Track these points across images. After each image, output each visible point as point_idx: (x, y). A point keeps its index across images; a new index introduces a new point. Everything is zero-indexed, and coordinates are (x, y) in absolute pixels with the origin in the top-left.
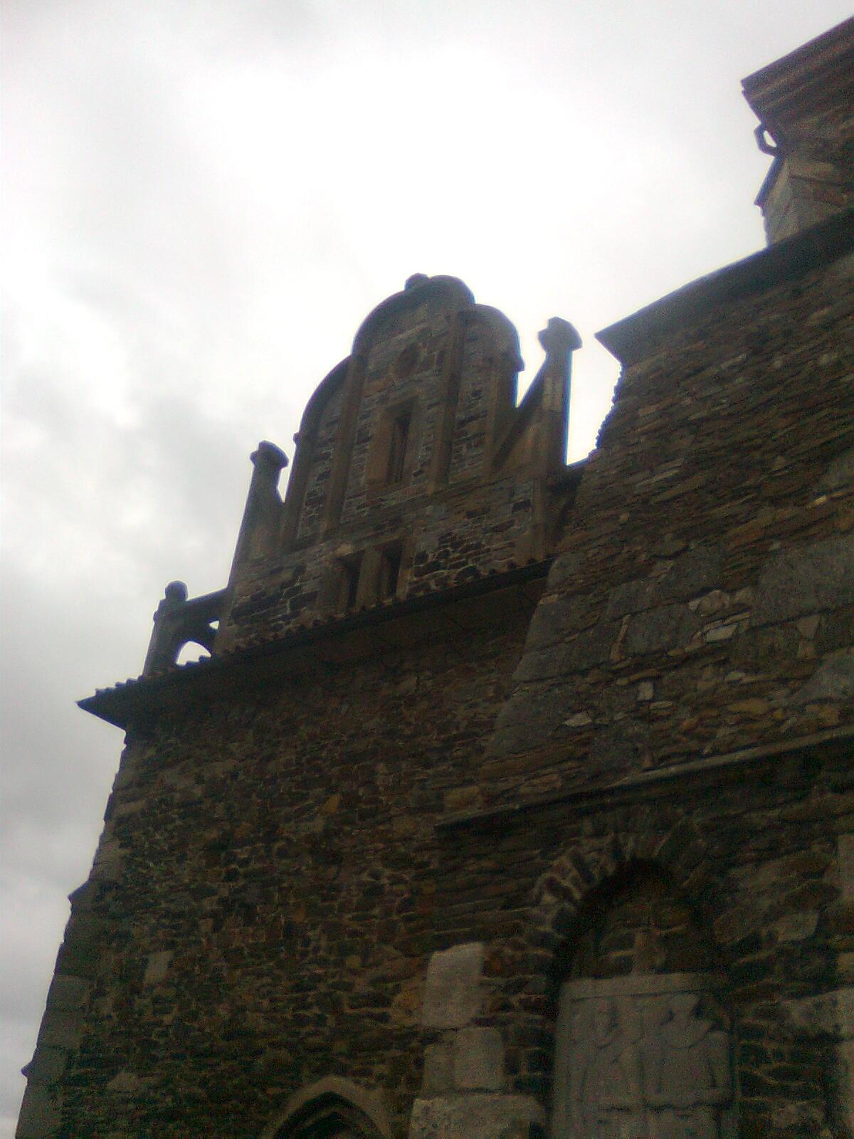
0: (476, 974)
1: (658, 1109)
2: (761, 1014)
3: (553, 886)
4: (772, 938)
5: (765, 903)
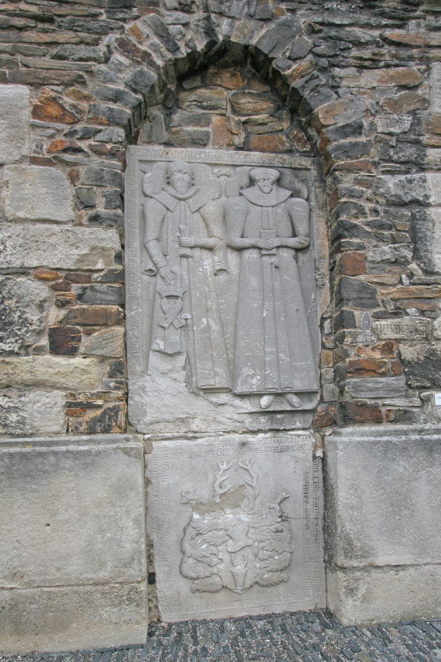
2: (358, 182)
4: (373, 127)
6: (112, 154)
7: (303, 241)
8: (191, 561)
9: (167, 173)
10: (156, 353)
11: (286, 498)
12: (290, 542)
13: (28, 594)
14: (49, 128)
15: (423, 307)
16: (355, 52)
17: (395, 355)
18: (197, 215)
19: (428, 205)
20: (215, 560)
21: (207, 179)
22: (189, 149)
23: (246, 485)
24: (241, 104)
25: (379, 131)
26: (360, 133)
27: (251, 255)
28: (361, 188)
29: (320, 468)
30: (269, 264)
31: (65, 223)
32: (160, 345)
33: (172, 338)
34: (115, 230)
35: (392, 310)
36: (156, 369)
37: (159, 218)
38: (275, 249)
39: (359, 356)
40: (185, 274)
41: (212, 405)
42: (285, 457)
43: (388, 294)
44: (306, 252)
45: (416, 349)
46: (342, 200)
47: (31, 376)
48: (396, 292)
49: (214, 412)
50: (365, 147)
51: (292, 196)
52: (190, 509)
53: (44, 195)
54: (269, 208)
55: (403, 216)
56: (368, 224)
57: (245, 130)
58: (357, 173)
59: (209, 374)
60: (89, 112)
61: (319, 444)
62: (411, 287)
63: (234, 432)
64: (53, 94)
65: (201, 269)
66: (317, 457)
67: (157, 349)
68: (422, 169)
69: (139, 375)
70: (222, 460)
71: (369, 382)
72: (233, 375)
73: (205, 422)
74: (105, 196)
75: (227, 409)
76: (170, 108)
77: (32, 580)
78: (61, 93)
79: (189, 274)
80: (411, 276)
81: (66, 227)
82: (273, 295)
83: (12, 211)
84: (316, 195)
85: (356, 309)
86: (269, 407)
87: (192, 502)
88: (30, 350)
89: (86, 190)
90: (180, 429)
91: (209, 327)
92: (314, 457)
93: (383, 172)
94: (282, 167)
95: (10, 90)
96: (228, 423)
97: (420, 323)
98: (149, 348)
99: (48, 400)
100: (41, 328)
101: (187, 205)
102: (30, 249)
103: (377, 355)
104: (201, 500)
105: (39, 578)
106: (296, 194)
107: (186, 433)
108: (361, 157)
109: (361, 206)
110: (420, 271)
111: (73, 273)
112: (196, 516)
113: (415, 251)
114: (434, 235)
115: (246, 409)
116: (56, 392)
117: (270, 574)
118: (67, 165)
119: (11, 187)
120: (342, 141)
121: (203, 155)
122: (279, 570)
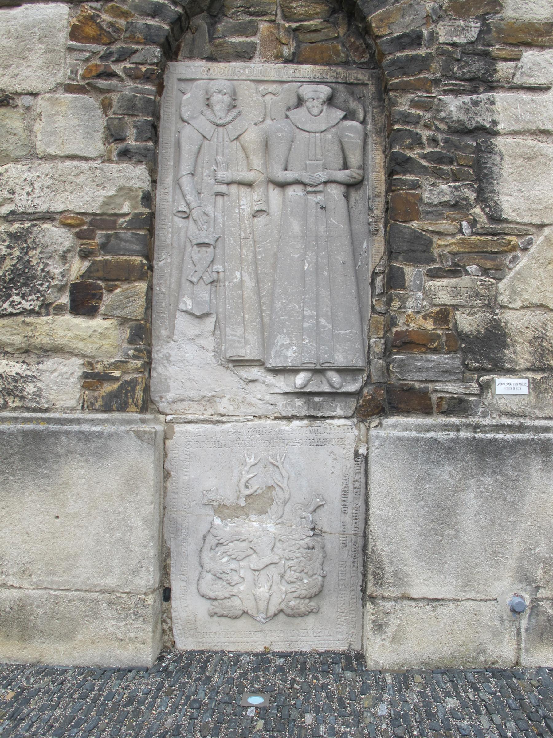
0: (63, 38)
2: (414, 104)
4: (433, 36)
6: (147, 78)
7: (355, 175)
8: (209, 576)
10: (183, 313)
11: (320, 506)
12: (323, 562)
13: (36, 596)
14: (85, 50)
15: (486, 264)
17: (451, 325)
18: (236, 144)
20: (235, 578)
21: (250, 99)
23: (275, 486)
24: (292, 7)
25: (441, 42)
26: (419, 45)
27: (295, 192)
28: (418, 112)
29: (363, 469)
30: (314, 204)
31: (94, 159)
32: (187, 303)
33: (200, 295)
34: (144, 166)
35: (450, 266)
36: (182, 333)
37: (195, 148)
38: (321, 185)
39: (408, 325)
40: (219, 215)
41: (242, 382)
42: (322, 452)
43: (446, 246)
44: (359, 189)
45: (476, 319)
46: (396, 127)
47: (50, 340)
48: (454, 243)
49: (243, 390)
50: (428, 58)
51: (345, 118)
52: (212, 513)
53: (75, 127)
54: (317, 134)
55: (467, 146)
56: (424, 157)
57: (296, 38)
58: (413, 93)
59: (239, 342)
60: (126, 30)
61: (363, 438)
62: (473, 237)
63: (266, 417)
64: (91, 12)
65: (237, 211)
66: (360, 455)
67: (185, 309)
68: (491, 87)
69: (164, 340)
70: (249, 452)
71: (418, 360)
72: (266, 344)
73: (234, 403)
74: (136, 126)
75: (258, 388)
78: (99, 10)
79: (223, 217)
80: (473, 223)
81: (95, 164)
82: (317, 243)
83: (43, 147)
84: (373, 116)
85: (407, 265)
86: (305, 386)
87: (214, 504)
89: (117, 121)
90: (205, 410)
91: (242, 281)
92: (356, 455)
93: (446, 92)
94: (335, 83)
95: (50, 10)
96: (259, 406)
97: (482, 285)
98: (176, 308)
99: (65, 369)
100: (63, 283)
101: (225, 132)
102: (57, 190)
103: (429, 325)
104: (224, 503)
106: (350, 115)
107: (212, 415)
108: (419, 73)
109: (417, 134)
110: (484, 217)
111: (98, 218)
112: (217, 521)
113: (480, 192)
114: (502, 172)
115: (279, 388)
116: (74, 359)
117: (298, 601)
118: (101, 92)
119: (43, 120)
120: (399, 54)
121: (247, 71)
122: (308, 597)
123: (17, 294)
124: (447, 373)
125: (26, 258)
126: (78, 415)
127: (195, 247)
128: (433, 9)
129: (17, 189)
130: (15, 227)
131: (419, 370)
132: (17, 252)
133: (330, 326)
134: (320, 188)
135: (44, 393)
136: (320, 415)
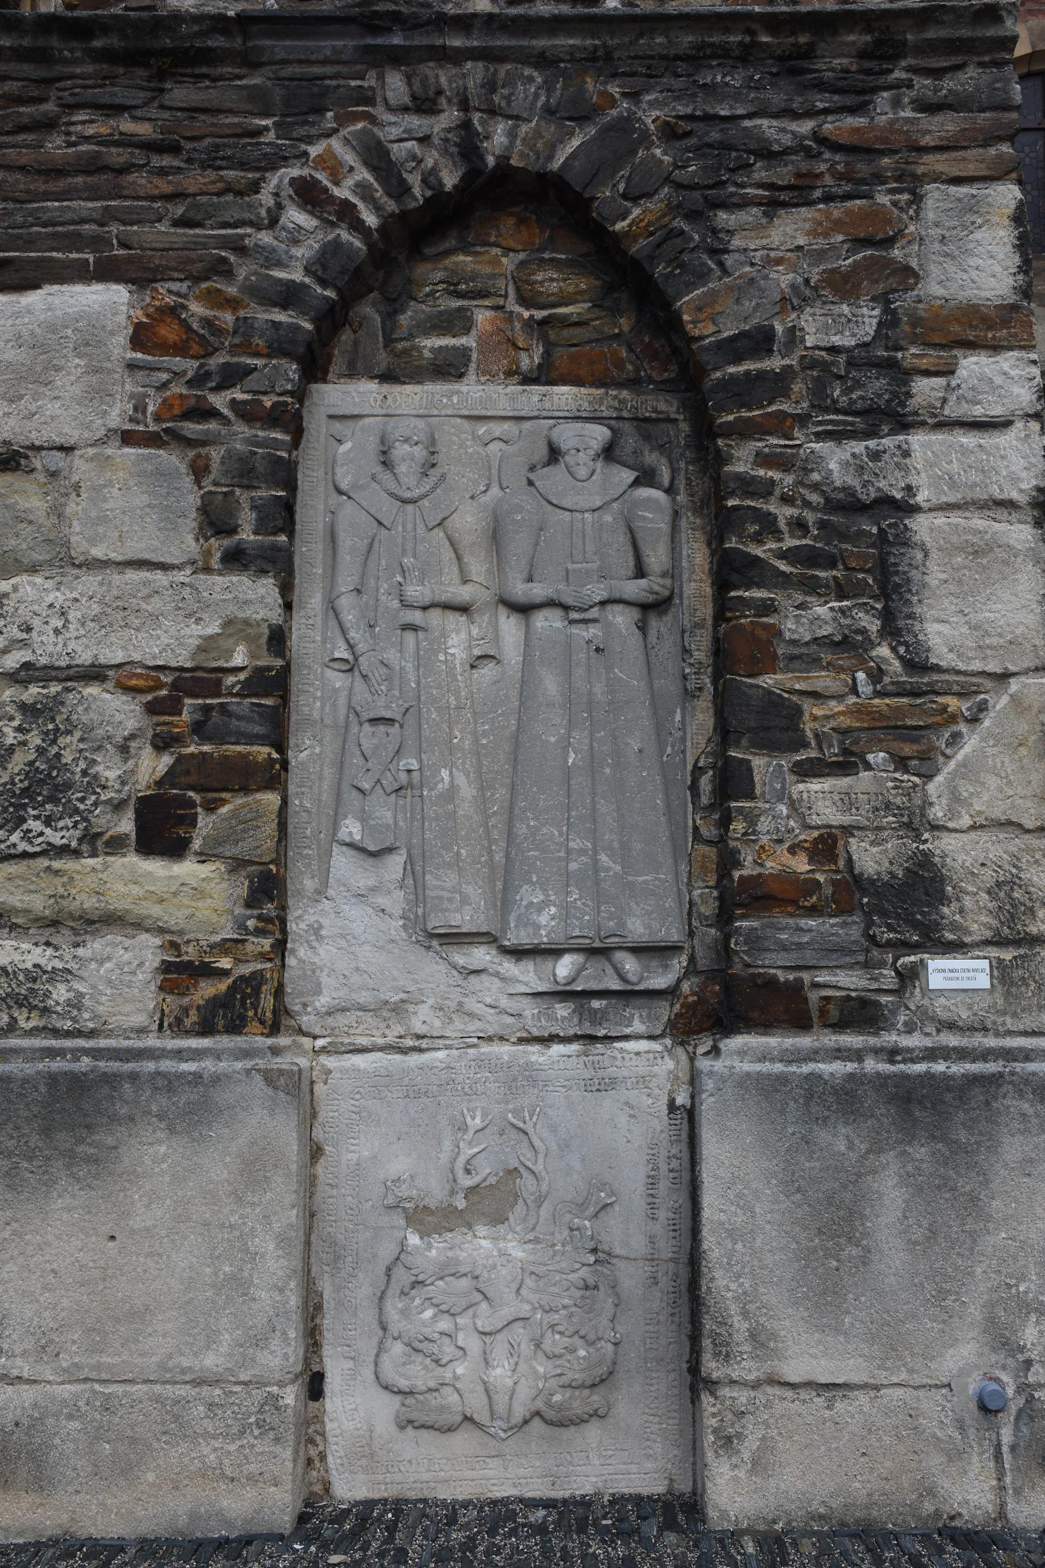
0: (119, 347)
1: (524, 609)
2: (764, 460)
3: (309, 194)
4: (794, 335)
5: (783, 279)
6: (274, 418)
8: (398, 1348)
9: (383, 442)
10: (344, 848)
11: (607, 1205)
12: (614, 1316)
13: (66, 1395)
14: (159, 369)
15: (902, 749)
16: (760, 173)
17: (841, 863)
19: (916, 509)
20: (448, 1350)
22: (430, 387)
23: (522, 1169)
25: (808, 345)
26: (770, 352)
28: (770, 474)
29: (684, 1135)
31: (179, 568)
32: (352, 829)
33: (378, 814)
34: (272, 581)
35: (836, 755)
36: (344, 885)
39: (761, 865)
40: (409, 667)
41: (455, 973)
42: (608, 1103)
43: (827, 717)
45: (886, 851)
46: (731, 503)
47: (99, 901)
48: (842, 713)
49: (459, 989)
52: (402, 1222)
53: (142, 509)
55: (862, 533)
56: (783, 555)
58: (760, 440)
59: (450, 900)
60: (235, 332)
62: (876, 701)
63: (502, 1038)
64: (170, 300)
65: (442, 657)
66: (678, 1108)
67: (348, 840)
68: (904, 424)
69: (309, 898)
70: (472, 1105)
71: (782, 929)
73: (441, 1013)
74: (256, 507)
75: (487, 984)
76: (395, 300)
77: (76, 1365)
78: (185, 296)
79: (417, 668)
80: (876, 675)
81: (182, 576)
83: (84, 546)
85: (756, 754)
86: (574, 980)
87: (408, 1205)
88: (99, 844)
89: (220, 497)
90: (388, 1027)
91: (453, 788)
92: (672, 1107)
93: (819, 436)
95: (95, 297)
96: (490, 1018)
97: (896, 788)
98: (333, 839)
99: (127, 956)
100: (123, 796)
102: (111, 625)
103: (801, 865)
104: (426, 1202)
105: (89, 1360)
107: (401, 1037)
108: (770, 404)
109: (770, 514)
110: (897, 663)
111: (188, 675)
112: (414, 1240)
113: (888, 616)
114: (927, 579)
115: (526, 984)
116: (144, 937)
117: (568, 1393)
118: (189, 444)
119: (84, 496)
120: (732, 369)
122: (587, 1383)
123: (36, 818)
124: (835, 952)
125: (54, 750)
126: (152, 1041)
127: (366, 725)
128: (793, 286)
129: (36, 622)
130: (33, 692)
131: (784, 948)
132: (35, 740)
133: (618, 868)
134: (594, 613)
135: (87, 1002)
136: (601, 1033)
